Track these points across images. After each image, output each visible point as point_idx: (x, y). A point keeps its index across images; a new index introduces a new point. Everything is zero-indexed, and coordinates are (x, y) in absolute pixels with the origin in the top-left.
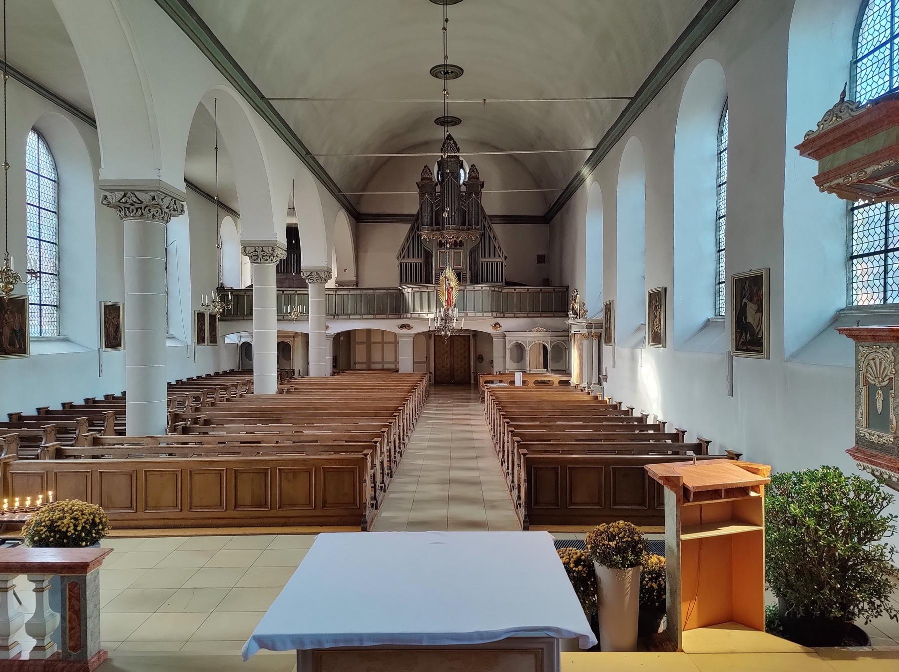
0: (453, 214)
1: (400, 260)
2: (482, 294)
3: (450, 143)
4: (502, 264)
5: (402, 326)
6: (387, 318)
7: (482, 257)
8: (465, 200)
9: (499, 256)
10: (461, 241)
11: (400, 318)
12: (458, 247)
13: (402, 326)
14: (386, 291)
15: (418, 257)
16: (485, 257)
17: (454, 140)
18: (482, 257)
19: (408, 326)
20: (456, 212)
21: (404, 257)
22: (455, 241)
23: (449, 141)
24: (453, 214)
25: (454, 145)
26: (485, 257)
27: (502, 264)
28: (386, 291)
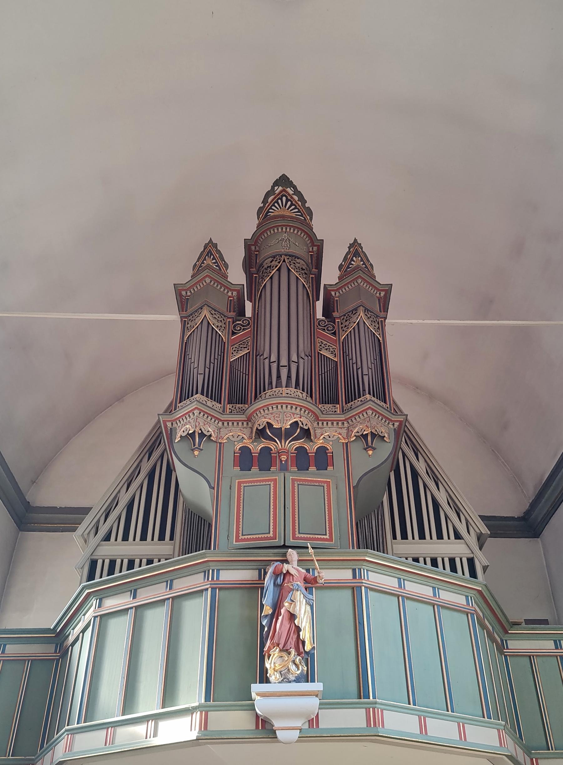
0: (294, 358)
2: (437, 621)
3: (284, 190)
4: (471, 561)
7: (395, 537)
8: (334, 334)
9: (458, 536)
10: (322, 450)
12: (312, 469)
15: (162, 537)
16: (404, 536)
17: (295, 187)
18: (395, 537)
24: (294, 358)
25: (296, 198)
27: (471, 561)
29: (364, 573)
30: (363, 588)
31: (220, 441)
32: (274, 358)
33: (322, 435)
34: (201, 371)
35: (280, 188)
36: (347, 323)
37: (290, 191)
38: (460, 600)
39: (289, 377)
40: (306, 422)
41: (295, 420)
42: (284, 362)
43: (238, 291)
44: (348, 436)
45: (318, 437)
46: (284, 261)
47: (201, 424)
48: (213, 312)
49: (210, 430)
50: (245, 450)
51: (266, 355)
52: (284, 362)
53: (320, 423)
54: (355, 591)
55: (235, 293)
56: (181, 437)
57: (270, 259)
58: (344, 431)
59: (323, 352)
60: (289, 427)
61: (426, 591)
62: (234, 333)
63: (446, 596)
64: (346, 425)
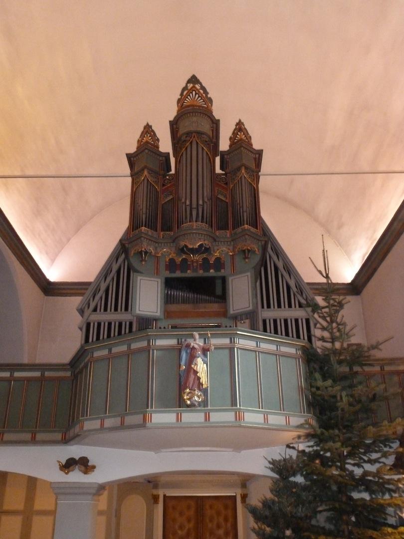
0: (201, 202)
1: (87, 312)
3: (194, 87)
5: (69, 465)
6: (34, 441)
8: (226, 184)
10: (218, 260)
11: (65, 441)
13: (69, 465)
14: (37, 374)
17: (201, 84)
19: (84, 464)
20: (206, 200)
21: (95, 310)
22: (206, 260)
23: (191, 85)
24: (201, 202)
26: (269, 306)
28: (37, 374)
29: (237, 340)
30: (236, 348)
31: (157, 255)
32: (188, 203)
33: (218, 250)
34: (144, 212)
35: (191, 85)
36: (234, 177)
37: (198, 86)
38: (292, 351)
39: (198, 214)
40: (207, 243)
41: (201, 243)
42: (194, 205)
43: (165, 157)
44: (234, 251)
45: (216, 251)
46: (194, 137)
47: (145, 246)
48: (150, 172)
49: (151, 249)
50: (172, 261)
51: (183, 200)
52: (194, 205)
53: (217, 243)
54: (231, 350)
55: (164, 158)
56: (134, 254)
57: (185, 135)
58: (231, 248)
59: (220, 196)
60: (197, 247)
61: (273, 347)
62: (164, 185)
63: (284, 349)
64: (232, 243)
